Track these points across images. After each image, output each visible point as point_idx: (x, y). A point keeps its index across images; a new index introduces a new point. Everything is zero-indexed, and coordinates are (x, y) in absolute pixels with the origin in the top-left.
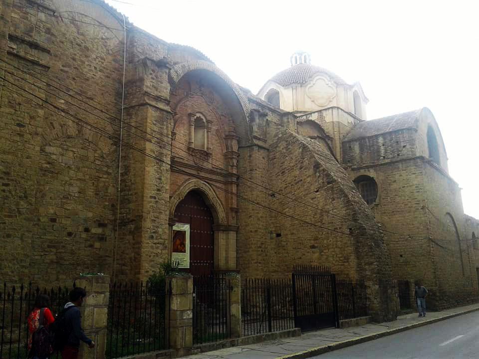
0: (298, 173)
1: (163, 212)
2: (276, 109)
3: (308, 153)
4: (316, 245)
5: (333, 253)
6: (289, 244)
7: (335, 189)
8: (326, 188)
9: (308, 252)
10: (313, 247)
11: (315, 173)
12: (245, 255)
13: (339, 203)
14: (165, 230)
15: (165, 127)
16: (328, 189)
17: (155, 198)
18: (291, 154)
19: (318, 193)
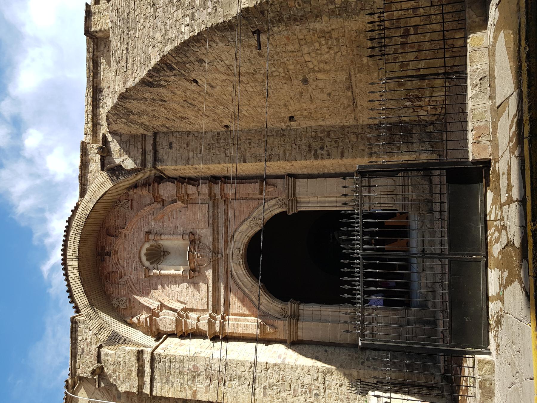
0: (173, 104)
1: (281, 373)
2: (91, 54)
3: (132, 93)
5: (313, 55)
8: (183, 72)
9: (316, 86)
10: (305, 81)
11: (162, 86)
12: (331, 168)
13: (206, 53)
14: (305, 371)
15: (172, 365)
17: (265, 388)
18: (146, 111)
19: (199, 81)
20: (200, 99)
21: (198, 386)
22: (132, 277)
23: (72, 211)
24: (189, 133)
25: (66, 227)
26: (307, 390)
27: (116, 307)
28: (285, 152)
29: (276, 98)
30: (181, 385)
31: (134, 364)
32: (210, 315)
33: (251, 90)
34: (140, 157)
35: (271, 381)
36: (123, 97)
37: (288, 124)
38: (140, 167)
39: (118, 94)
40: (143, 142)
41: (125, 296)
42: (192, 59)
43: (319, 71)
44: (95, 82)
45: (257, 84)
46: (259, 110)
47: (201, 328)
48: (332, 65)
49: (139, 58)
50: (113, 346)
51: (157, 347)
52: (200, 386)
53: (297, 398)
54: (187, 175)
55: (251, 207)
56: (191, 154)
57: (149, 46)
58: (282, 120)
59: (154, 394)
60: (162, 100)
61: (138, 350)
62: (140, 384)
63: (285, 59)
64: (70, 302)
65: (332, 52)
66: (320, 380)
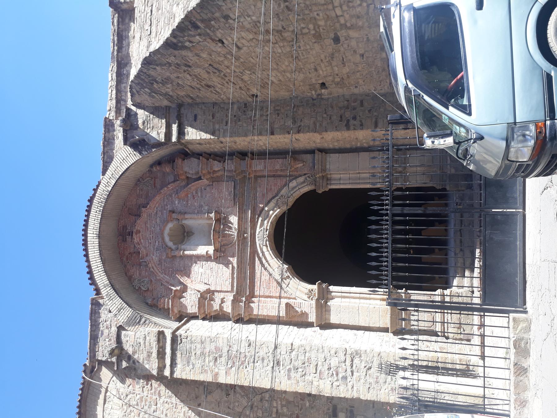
0: (198, 69)
1: (307, 354)
3: (155, 58)
4: (332, 35)
5: (345, 8)
6: (337, 72)
7: (205, 17)
8: (208, 31)
9: (348, 46)
10: (337, 40)
11: (185, 48)
12: (364, 141)
16: (209, 27)
17: (289, 370)
18: (170, 78)
19: (224, 41)
20: (226, 63)
21: (220, 368)
22: (154, 257)
23: (94, 190)
24: (215, 104)
25: (88, 206)
26: (334, 373)
27: (137, 288)
28: (315, 124)
29: (306, 60)
30: (202, 367)
31: (154, 346)
32: (234, 295)
33: (280, 51)
34: (164, 131)
35: (296, 364)
36: (147, 62)
37: (319, 92)
38: (163, 140)
39: (141, 60)
40: (168, 114)
41: (146, 278)
42: (217, 15)
43: (352, 27)
44: (119, 57)
45: (285, 44)
46: (288, 75)
47: (225, 309)
48: (365, 20)
49: (163, 19)
50: (133, 327)
51: (178, 328)
52: (222, 368)
53: (323, 381)
54: (212, 150)
55: (279, 184)
56: (217, 127)
57: (173, 5)
58: (312, 87)
59: (175, 376)
60: (186, 65)
61: (159, 331)
62: (161, 365)
63: (315, 13)
64: (90, 284)
65: (365, 4)
66: (348, 363)
